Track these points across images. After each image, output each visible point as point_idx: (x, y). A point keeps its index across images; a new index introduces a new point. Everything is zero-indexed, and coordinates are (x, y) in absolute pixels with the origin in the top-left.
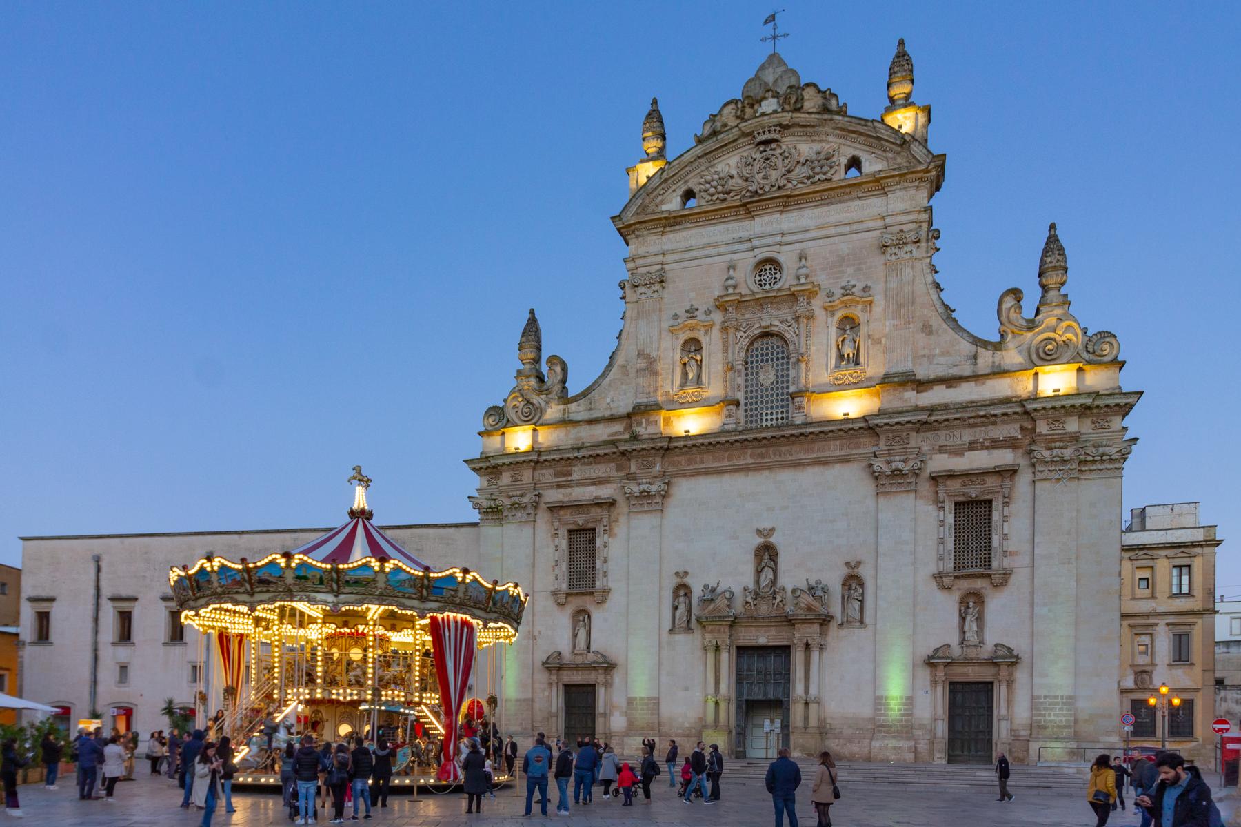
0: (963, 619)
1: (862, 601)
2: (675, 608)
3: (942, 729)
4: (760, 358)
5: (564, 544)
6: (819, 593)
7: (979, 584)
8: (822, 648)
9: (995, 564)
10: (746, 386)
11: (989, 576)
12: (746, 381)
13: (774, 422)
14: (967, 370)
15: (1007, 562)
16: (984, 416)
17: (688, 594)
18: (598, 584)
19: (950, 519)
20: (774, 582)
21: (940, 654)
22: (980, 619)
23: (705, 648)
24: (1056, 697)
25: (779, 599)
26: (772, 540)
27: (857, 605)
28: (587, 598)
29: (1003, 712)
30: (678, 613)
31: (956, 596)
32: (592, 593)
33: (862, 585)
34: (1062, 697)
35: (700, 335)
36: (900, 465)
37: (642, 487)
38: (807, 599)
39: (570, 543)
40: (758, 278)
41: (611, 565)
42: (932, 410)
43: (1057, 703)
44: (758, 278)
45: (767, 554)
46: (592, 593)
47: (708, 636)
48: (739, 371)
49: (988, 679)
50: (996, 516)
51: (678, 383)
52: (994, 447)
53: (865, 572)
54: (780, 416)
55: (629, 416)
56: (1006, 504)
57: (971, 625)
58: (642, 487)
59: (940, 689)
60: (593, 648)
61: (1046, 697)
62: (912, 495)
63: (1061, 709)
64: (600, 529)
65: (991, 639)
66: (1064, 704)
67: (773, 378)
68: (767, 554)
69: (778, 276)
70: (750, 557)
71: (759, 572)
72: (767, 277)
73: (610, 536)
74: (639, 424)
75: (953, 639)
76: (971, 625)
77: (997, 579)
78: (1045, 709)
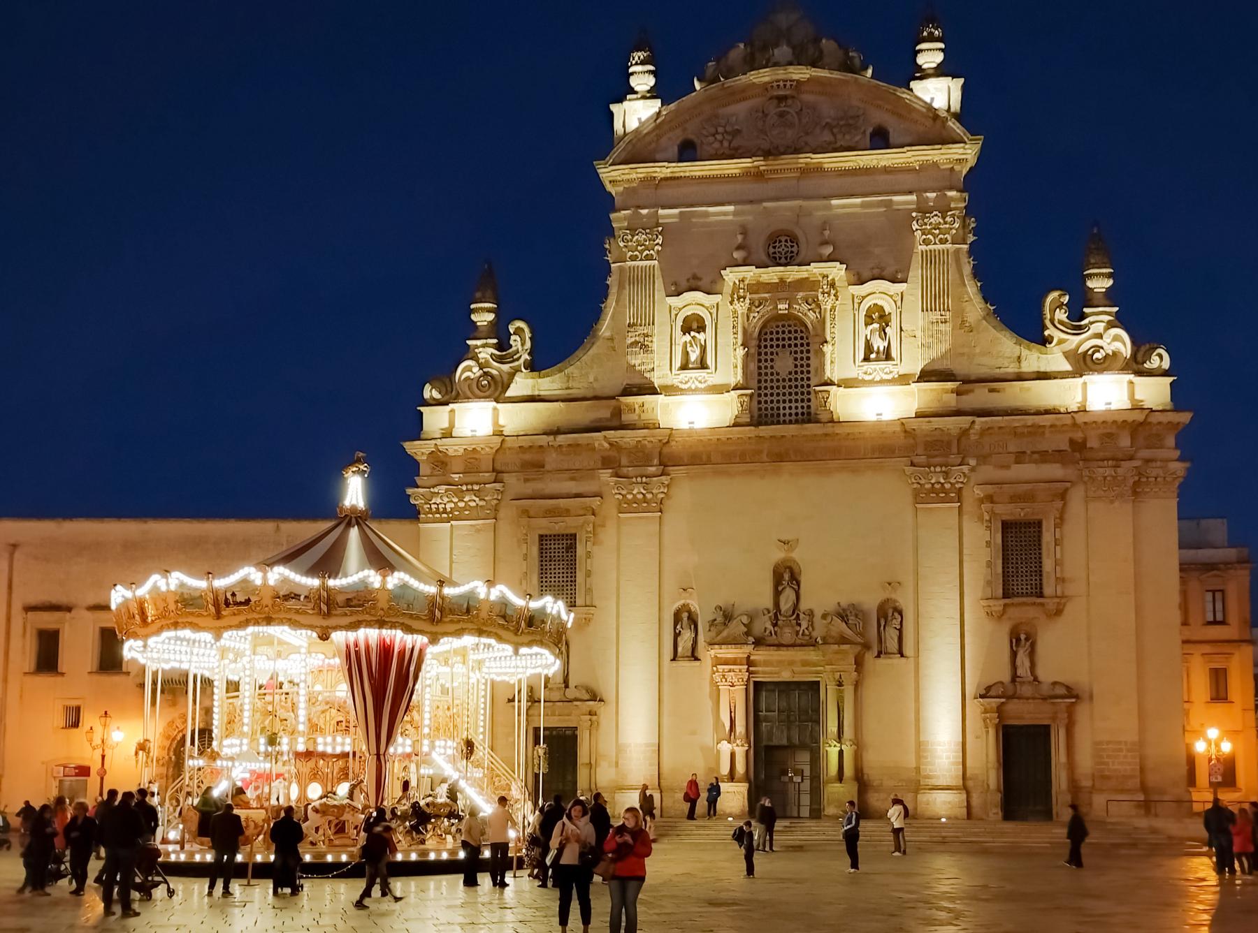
0: (1014, 655)
1: (900, 631)
3: (993, 778)
4: (775, 343)
6: (852, 620)
7: (1031, 612)
8: (857, 685)
9: (1048, 590)
10: (760, 374)
11: (1042, 605)
12: (760, 368)
13: (793, 417)
14: (1012, 369)
17: (693, 621)
20: (796, 606)
21: (992, 693)
22: (1032, 654)
24: (1120, 743)
25: (804, 624)
26: (795, 555)
27: (895, 634)
29: (1063, 758)
33: (901, 613)
34: (1126, 743)
40: (771, 250)
43: (1120, 750)
44: (771, 250)
45: (786, 577)
49: (1046, 722)
50: (1047, 537)
51: (679, 365)
52: (1044, 461)
54: (800, 411)
57: (1023, 659)
59: (992, 732)
60: (572, 683)
61: (1108, 743)
63: (1125, 757)
65: (1047, 673)
66: (1128, 751)
67: (792, 369)
68: (786, 577)
69: (795, 249)
70: (769, 577)
71: (777, 593)
75: (1006, 678)
76: (1023, 659)
77: (1051, 604)
78: (1108, 756)
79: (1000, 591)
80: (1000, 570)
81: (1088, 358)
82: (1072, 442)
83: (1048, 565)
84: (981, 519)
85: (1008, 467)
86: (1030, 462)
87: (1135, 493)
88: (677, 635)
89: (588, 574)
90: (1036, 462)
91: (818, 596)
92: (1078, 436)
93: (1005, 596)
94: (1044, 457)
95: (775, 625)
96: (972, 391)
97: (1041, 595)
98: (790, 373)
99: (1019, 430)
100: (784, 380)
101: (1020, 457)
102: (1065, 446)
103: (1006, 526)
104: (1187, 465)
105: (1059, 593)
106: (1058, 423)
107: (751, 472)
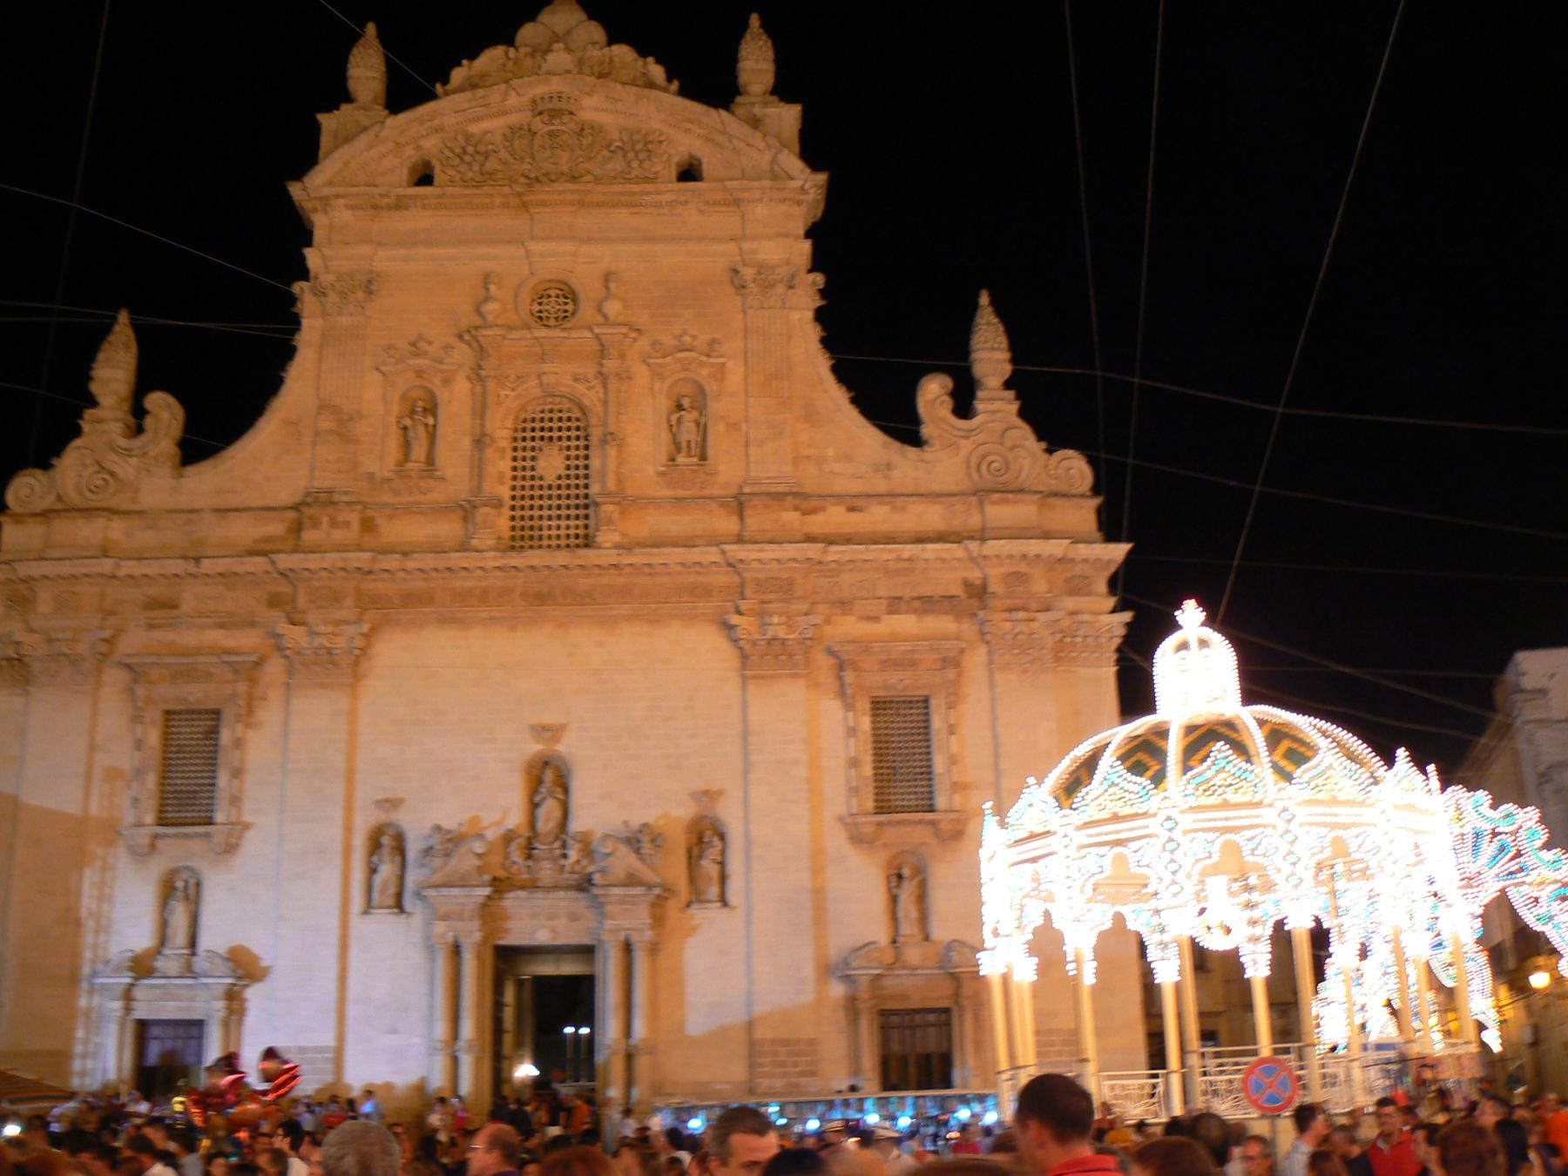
1: (722, 864)
2: (373, 870)
5: (154, 737)
6: (647, 848)
7: (919, 835)
8: (654, 949)
9: (941, 801)
11: (933, 823)
14: (881, 486)
15: (957, 800)
16: (910, 559)
17: (400, 849)
18: (220, 817)
19: (866, 723)
22: (922, 898)
23: (430, 949)
26: (561, 748)
28: (196, 845)
30: (378, 879)
31: (882, 856)
32: (207, 835)
33: (722, 837)
35: (435, 384)
36: (782, 633)
37: (318, 641)
38: (624, 860)
39: (167, 736)
41: (250, 784)
42: (830, 540)
45: (548, 778)
46: (207, 835)
47: (440, 927)
48: (503, 450)
50: (937, 723)
52: (926, 612)
53: (730, 814)
55: (295, 508)
56: (951, 706)
58: (318, 641)
62: (801, 683)
64: (228, 714)
68: (548, 778)
69: (570, 307)
72: (552, 306)
73: (248, 726)
74: (316, 524)
79: (870, 805)
80: (868, 770)
81: (984, 468)
82: (967, 584)
83: (939, 763)
84: (842, 693)
85: (876, 619)
86: (907, 612)
87: (1058, 659)
88: (373, 870)
89: (237, 773)
90: (915, 611)
91: (595, 812)
92: (975, 575)
93: (879, 810)
94: (927, 604)
95: (529, 857)
96: (823, 509)
97: (931, 809)
98: (560, 478)
99: (892, 565)
100: (550, 487)
101: (895, 605)
102: (957, 590)
103: (879, 706)
104: (1127, 616)
105: (957, 805)
106: (945, 556)
107: (494, 620)
